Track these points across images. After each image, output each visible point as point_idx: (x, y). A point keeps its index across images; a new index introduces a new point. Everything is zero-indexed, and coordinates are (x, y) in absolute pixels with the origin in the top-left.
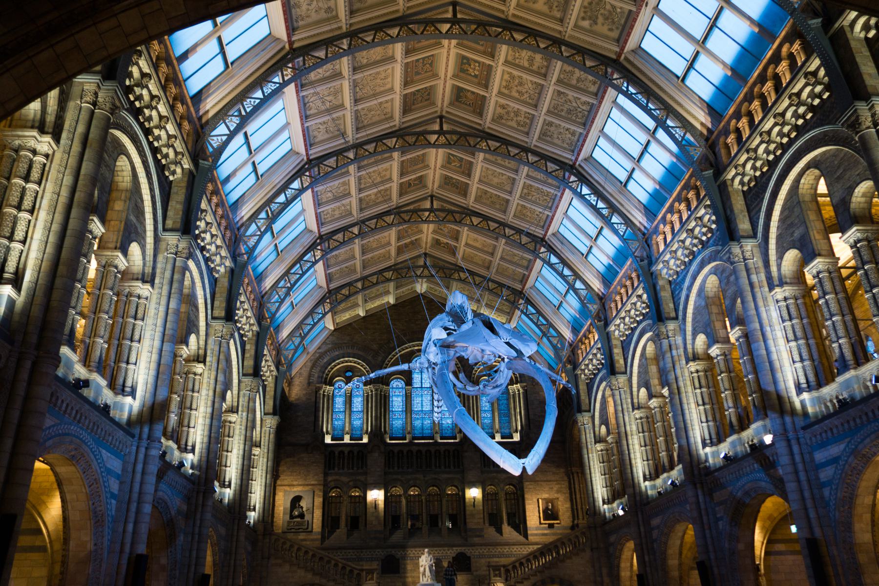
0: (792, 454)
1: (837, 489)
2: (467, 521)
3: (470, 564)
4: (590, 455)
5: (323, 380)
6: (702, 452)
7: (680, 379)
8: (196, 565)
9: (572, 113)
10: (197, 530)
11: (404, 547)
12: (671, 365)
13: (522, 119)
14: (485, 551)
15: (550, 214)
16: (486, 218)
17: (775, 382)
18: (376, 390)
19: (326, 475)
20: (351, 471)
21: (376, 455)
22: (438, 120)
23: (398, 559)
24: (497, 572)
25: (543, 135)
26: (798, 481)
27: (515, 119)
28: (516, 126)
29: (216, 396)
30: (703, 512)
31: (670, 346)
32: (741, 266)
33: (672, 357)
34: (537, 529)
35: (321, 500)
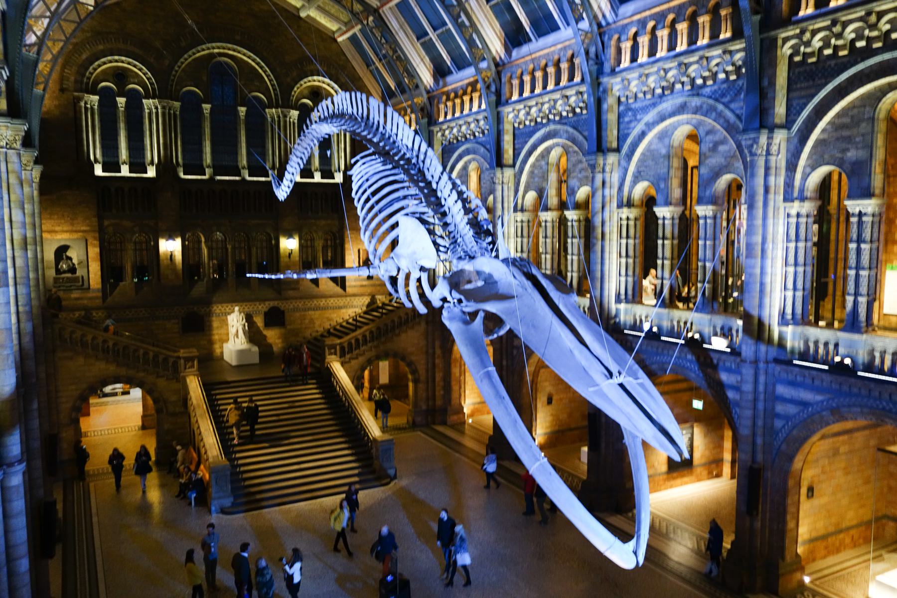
0: (756, 381)
1: (794, 428)
5: (84, 86)
6: (613, 307)
7: (607, 224)
11: (208, 303)
12: (600, 205)
14: (300, 304)
17: (761, 306)
18: (163, 108)
19: (100, 218)
24: (333, 351)
26: (755, 408)
29: (16, 247)
31: (604, 183)
32: (761, 162)
33: (603, 197)
35: (97, 250)
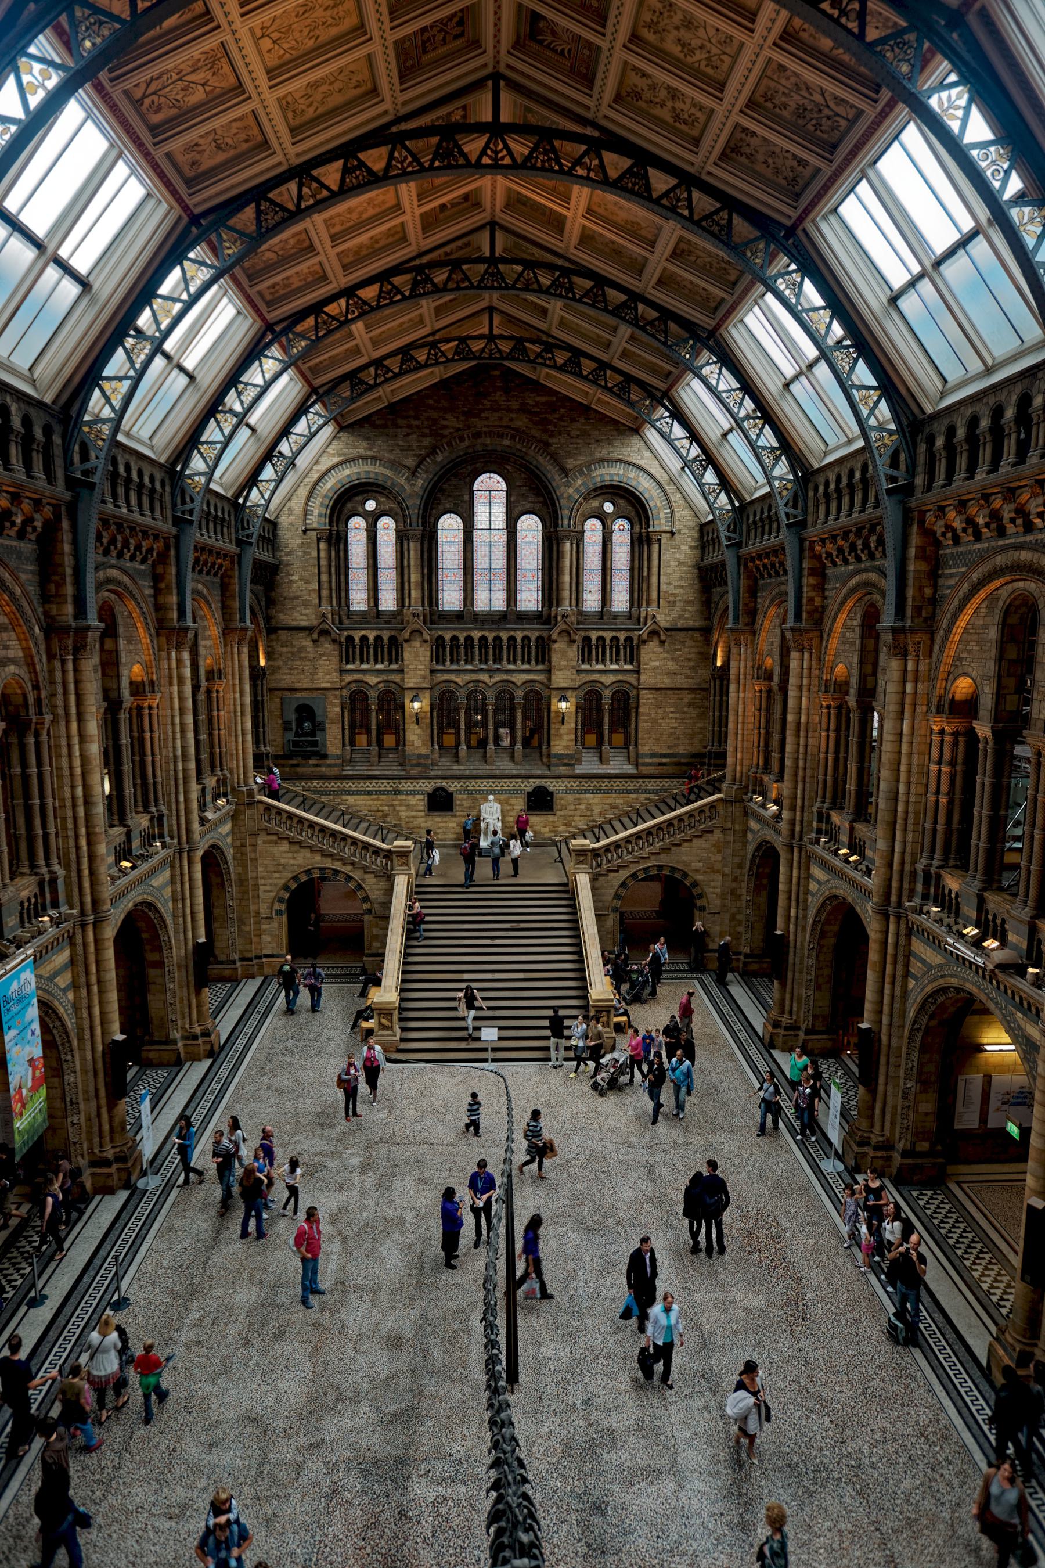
3: (552, 800)
4: (741, 695)
8: (102, 1024)
9: (808, 115)
10: (93, 979)
13: (686, 107)
15: (730, 300)
16: (602, 281)
20: (379, 666)
21: (417, 644)
22: (490, 83)
23: (451, 794)
25: (732, 152)
27: (669, 104)
28: (671, 121)
30: (889, 959)
34: (653, 755)
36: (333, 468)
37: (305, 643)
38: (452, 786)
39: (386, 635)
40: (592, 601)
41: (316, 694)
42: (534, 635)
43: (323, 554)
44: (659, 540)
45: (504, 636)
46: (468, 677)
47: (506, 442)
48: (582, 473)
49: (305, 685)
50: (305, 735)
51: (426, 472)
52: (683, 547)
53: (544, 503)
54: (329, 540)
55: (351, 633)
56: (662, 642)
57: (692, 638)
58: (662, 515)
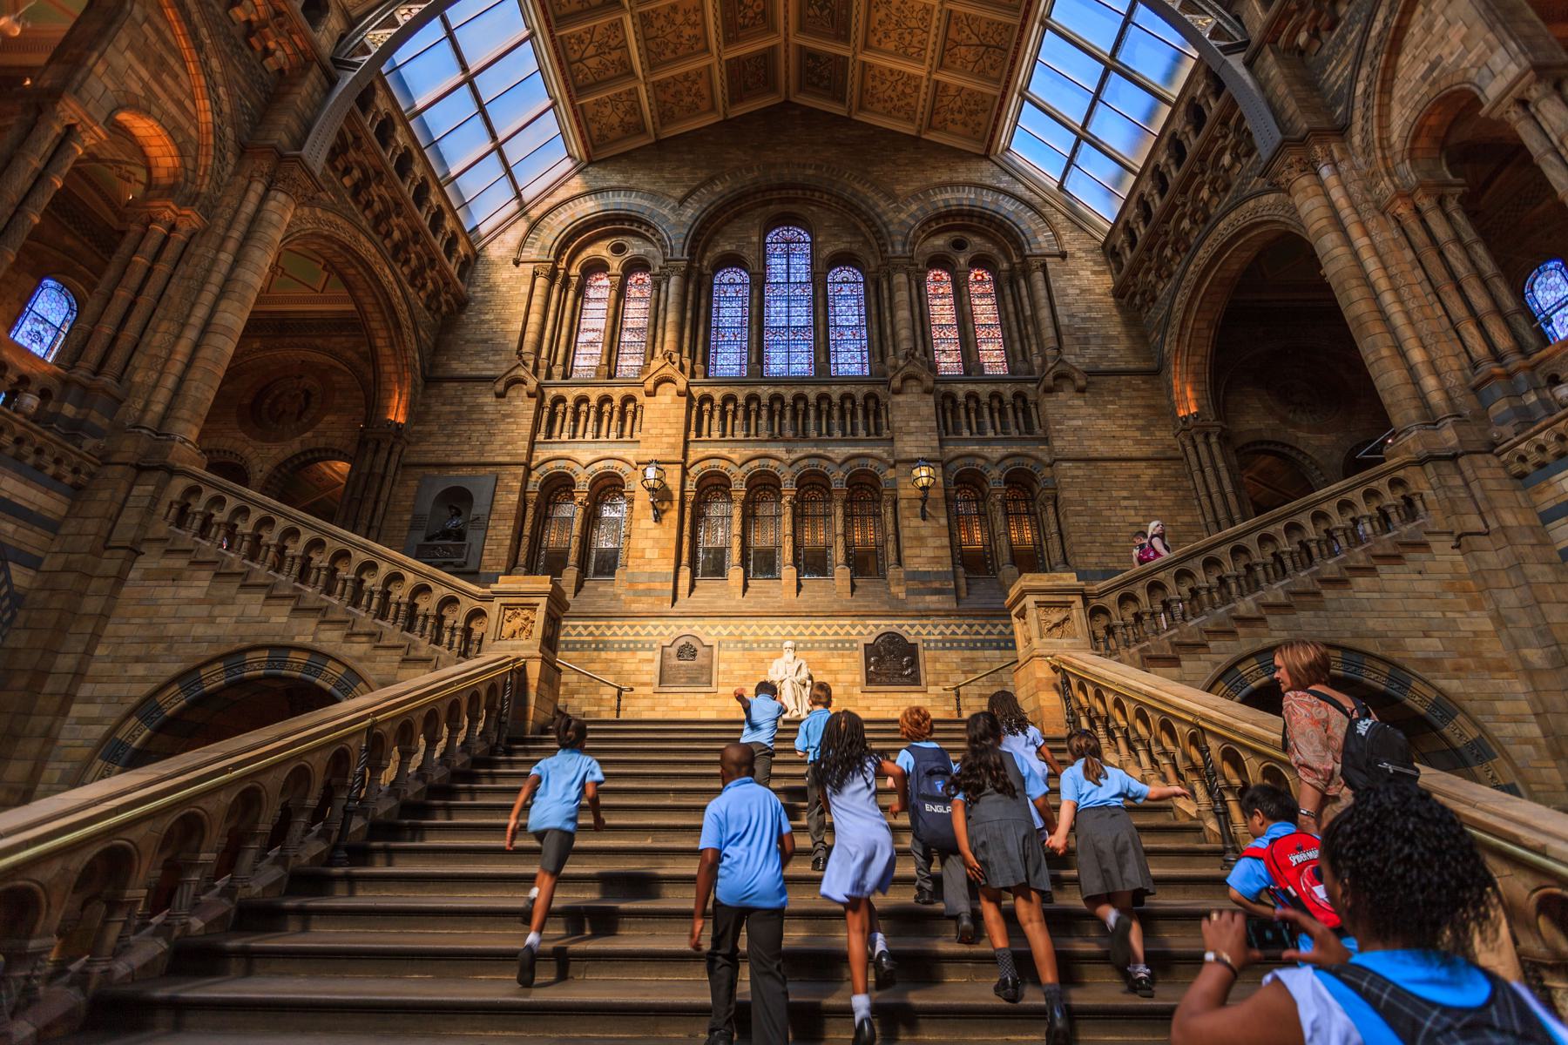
2: (906, 553)
3: (914, 662)
4: (1361, 242)
36: (572, 199)
37: (482, 400)
38: (709, 632)
39: (617, 394)
40: (948, 362)
41: (482, 471)
42: (860, 392)
43: (538, 291)
44: (1044, 266)
45: (811, 393)
46: (750, 452)
47: (810, 172)
48: (915, 197)
49: (467, 460)
50: (446, 534)
51: (700, 201)
52: (1081, 273)
53: (867, 242)
54: (552, 277)
55: (561, 391)
56: (1081, 390)
57: (1129, 385)
58: (1040, 238)
